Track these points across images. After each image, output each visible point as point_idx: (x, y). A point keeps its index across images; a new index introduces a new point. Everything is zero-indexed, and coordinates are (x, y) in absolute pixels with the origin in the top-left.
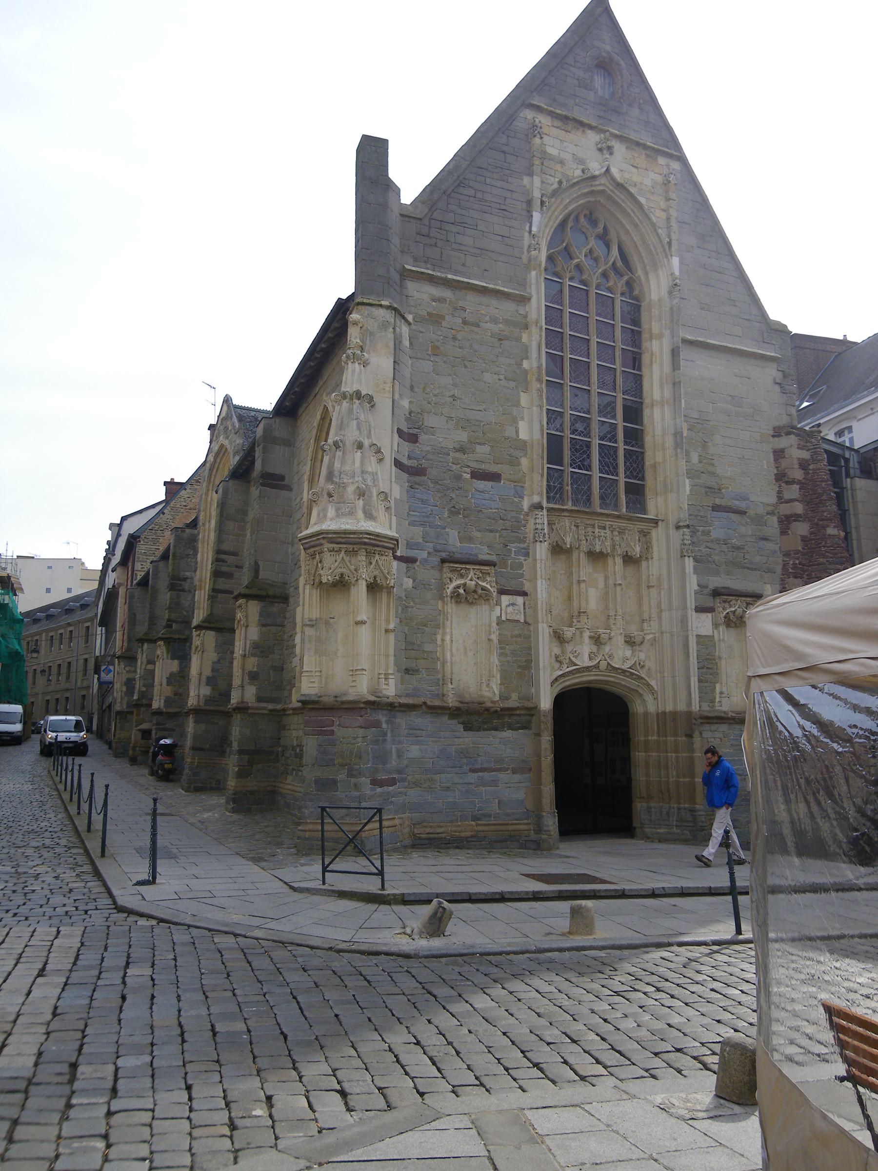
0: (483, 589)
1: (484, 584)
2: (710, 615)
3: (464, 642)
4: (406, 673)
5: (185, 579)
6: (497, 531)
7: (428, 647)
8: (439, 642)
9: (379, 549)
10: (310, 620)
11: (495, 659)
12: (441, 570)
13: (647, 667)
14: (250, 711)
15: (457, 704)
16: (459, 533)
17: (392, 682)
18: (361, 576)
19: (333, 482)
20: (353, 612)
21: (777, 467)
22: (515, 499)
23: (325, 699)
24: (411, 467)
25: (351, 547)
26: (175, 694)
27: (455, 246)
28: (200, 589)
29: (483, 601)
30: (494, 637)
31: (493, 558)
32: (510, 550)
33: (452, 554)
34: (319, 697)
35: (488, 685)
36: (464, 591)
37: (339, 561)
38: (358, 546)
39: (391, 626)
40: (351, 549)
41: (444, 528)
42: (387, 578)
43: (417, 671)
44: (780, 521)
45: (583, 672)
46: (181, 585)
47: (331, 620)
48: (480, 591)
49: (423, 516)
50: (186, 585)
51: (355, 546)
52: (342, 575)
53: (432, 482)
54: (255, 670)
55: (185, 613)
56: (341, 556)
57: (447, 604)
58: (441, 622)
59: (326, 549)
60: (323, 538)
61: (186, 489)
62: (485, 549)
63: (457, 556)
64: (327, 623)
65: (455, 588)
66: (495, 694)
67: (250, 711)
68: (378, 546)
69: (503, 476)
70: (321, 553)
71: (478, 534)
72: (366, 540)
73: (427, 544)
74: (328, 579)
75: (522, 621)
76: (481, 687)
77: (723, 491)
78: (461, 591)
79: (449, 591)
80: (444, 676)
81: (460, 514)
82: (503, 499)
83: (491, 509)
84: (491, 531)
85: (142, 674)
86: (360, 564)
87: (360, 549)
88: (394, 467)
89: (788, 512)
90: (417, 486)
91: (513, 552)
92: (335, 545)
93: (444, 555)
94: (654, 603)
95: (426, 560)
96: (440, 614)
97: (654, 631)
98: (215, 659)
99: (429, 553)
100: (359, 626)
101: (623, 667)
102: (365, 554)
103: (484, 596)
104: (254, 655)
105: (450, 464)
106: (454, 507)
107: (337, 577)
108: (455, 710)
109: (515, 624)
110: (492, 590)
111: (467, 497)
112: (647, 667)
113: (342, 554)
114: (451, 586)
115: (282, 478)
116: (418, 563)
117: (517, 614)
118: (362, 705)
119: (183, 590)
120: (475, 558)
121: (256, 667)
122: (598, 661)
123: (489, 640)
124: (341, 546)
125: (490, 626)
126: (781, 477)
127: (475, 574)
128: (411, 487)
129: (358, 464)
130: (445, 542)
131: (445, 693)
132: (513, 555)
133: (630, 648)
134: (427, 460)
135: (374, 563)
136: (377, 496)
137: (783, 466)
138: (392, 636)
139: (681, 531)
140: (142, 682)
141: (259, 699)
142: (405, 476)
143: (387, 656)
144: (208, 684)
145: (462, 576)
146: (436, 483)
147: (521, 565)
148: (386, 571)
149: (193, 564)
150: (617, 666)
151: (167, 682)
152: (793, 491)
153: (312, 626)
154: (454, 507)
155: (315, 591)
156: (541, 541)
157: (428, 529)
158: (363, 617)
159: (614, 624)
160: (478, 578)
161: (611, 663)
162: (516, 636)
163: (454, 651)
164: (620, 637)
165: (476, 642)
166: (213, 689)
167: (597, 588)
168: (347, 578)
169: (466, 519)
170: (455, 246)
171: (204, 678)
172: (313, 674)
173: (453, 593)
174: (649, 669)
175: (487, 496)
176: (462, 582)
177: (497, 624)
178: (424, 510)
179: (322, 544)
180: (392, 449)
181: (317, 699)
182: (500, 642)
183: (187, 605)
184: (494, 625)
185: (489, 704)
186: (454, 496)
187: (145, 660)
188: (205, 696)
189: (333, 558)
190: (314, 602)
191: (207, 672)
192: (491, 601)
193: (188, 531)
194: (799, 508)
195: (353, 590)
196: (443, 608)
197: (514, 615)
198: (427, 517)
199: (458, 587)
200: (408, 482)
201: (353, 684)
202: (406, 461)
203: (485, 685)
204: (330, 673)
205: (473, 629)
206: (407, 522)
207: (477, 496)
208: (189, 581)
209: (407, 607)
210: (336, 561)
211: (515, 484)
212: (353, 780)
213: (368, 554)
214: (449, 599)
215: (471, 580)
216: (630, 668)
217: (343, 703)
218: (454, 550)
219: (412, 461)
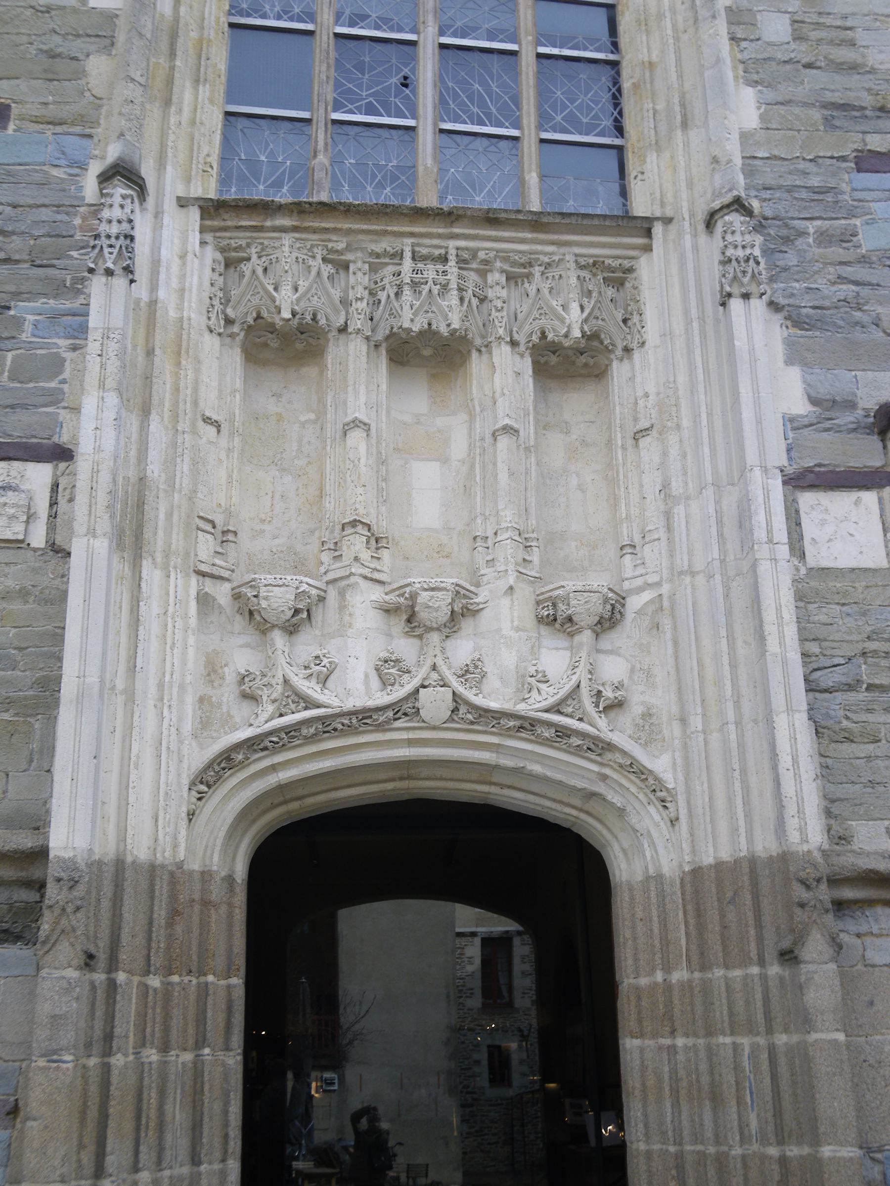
2: (869, 498)
13: (636, 710)
22: (55, 172)
45: (350, 730)
69: (15, 110)
75: (38, 538)
91: (28, 327)
94: (652, 482)
97: (653, 579)
101: (521, 708)
112: (636, 710)
122: (408, 688)
133: (566, 644)
147: (56, 365)
150: (494, 705)
156: (109, 273)
159: (491, 562)
161: (469, 695)
164: (505, 602)
167: (444, 460)
174: (647, 715)
211: (59, 129)
216: (556, 709)
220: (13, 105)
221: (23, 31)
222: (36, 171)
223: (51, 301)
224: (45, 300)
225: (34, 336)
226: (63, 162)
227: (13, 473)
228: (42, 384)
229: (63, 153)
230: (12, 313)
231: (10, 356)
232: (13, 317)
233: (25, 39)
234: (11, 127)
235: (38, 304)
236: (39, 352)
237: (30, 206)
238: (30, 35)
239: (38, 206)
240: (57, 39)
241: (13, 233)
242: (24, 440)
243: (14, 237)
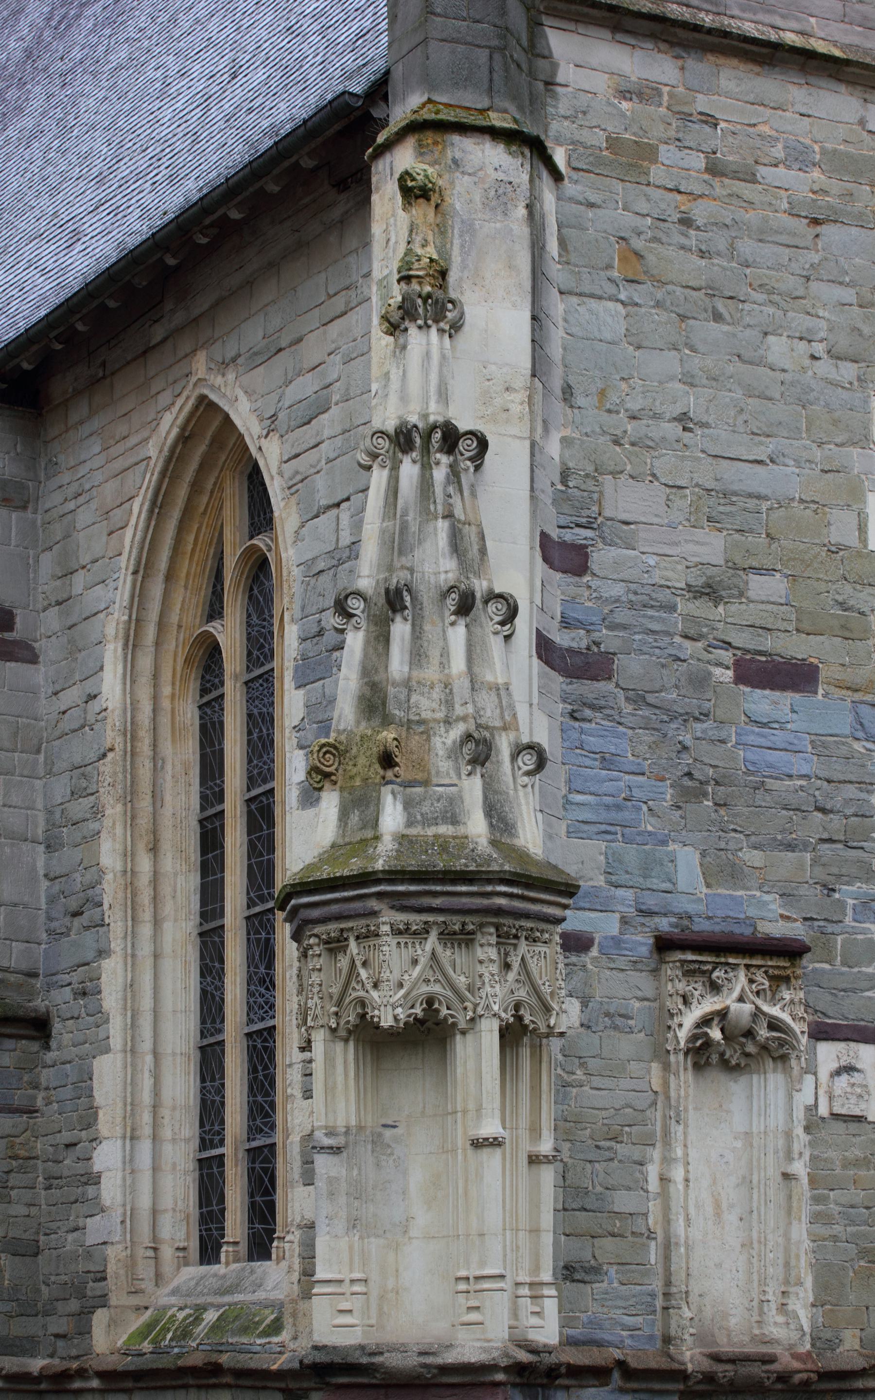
0: (774, 1025)
1: (775, 1011)
3: (714, 1182)
4: (565, 1278)
6: (805, 846)
7: (623, 1201)
8: (653, 1185)
9: (529, 924)
10: (331, 1133)
11: (800, 1231)
12: (655, 971)
15: (707, 1365)
16: (703, 854)
17: (551, 1306)
18: (488, 1007)
19: (387, 721)
20: (465, 1112)
22: (857, 746)
24: (570, 650)
29: (770, 1064)
30: (800, 1168)
31: (797, 930)
32: (842, 904)
33: (686, 922)
34: (373, 1354)
35: (782, 1308)
36: (722, 1030)
37: (423, 961)
38: (477, 919)
39: (546, 1147)
40: (457, 928)
41: (664, 843)
42: (548, 1009)
43: (595, 1271)
47: (388, 1133)
48: (763, 1033)
49: (607, 807)
51: (467, 919)
52: (430, 1001)
53: (627, 699)
56: (428, 947)
57: (677, 1074)
58: (658, 1128)
59: (386, 928)
60: (380, 895)
62: (774, 905)
63: (702, 926)
64: (377, 1141)
65: (698, 1025)
66: (804, 1335)
68: (527, 916)
69: (823, 675)
70: (368, 936)
71: (754, 857)
72: (502, 901)
73: (620, 892)
74: (396, 1018)
76: (761, 1313)
78: (716, 1034)
79: (683, 1035)
80: (668, 1283)
81: (705, 795)
82: (824, 745)
83: (790, 776)
84: (790, 847)
86: (481, 969)
87: (482, 926)
88: (535, 660)
90: (588, 713)
91: (849, 911)
93: (664, 924)
95: (617, 942)
96: (654, 1103)
99: (624, 921)
100: (486, 1151)
102: (493, 940)
103: (773, 1045)
105: (678, 639)
106: (689, 774)
107: (418, 1011)
108: (699, 1382)
109: (853, 1127)
110: (797, 1027)
111: (723, 742)
113: (432, 940)
114: (690, 1018)
116: (594, 952)
117: (860, 1096)
118: (500, 1377)
123: (786, 1176)
124: (431, 918)
125: (789, 1135)
127: (751, 981)
128: (572, 715)
129: (458, 664)
130: (667, 886)
131: (673, 1333)
132: (848, 920)
134: (612, 627)
135: (516, 966)
136: (514, 757)
138: (548, 1175)
142: (558, 681)
143: (535, 1231)
145: (715, 988)
146: (638, 699)
148: (546, 990)
153: (335, 1150)
154: (689, 774)
155: (339, 1046)
157: (618, 845)
158: (491, 1128)
160: (758, 993)
162: (856, 1163)
163: (692, 1211)
165: (746, 1182)
168: (444, 1012)
169: (722, 812)
172: (345, 1288)
173: (694, 1038)
175: (779, 738)
176: (718, 1007)
177: (807, 1129)
178: (608, 787)
179: (374, 914)
180: (532, 602)
181: (364, 1360)
182: (813, 1181)
184: (799, 1131)
185: (786, 1362)
186: (688, 740)
189: (407, 954)
190: (340, 1079)
192: (793, 1062)
195: (462, 1047)
196: (666, 1084)
197: (854, 1099)
198: (618, 807)
199: (706, 1021)
200: (564, 701)
201: (474, 1317)
202: (561, 639)
203: (773, 1306)
204: (391, 1284)
205: (739, 1144)
206: (564, 828)
207: (751, 739)
209: (566, 1085)
210: (415, 962)
211: (858, 696)
213: (505, 939)
214: (681, 1057)
215: (741, 999)
217: (445, 1369)
218: (691, 908)
219: (573, 633)
220: (820, 665)
221: (821, 576)
222: (843, 744)
223: (864, 886)
224: (859, 884)
225: (855, 920)
226: (860, 734)
227: (851, 1053)
228: (864, 969)
229: (861, 724)
230: (837, 896)
231: (839, 939)
232: (839, 900)
233: (822, 587)
234: (821, 691)
235: (854, 888)
236: (860, 937)
237: (840, 782)
238: (827, 582)
239: (845, 782)
240: (848, 588)
241: (831, 811)
242: (856, 1023)
243: (832, 816)
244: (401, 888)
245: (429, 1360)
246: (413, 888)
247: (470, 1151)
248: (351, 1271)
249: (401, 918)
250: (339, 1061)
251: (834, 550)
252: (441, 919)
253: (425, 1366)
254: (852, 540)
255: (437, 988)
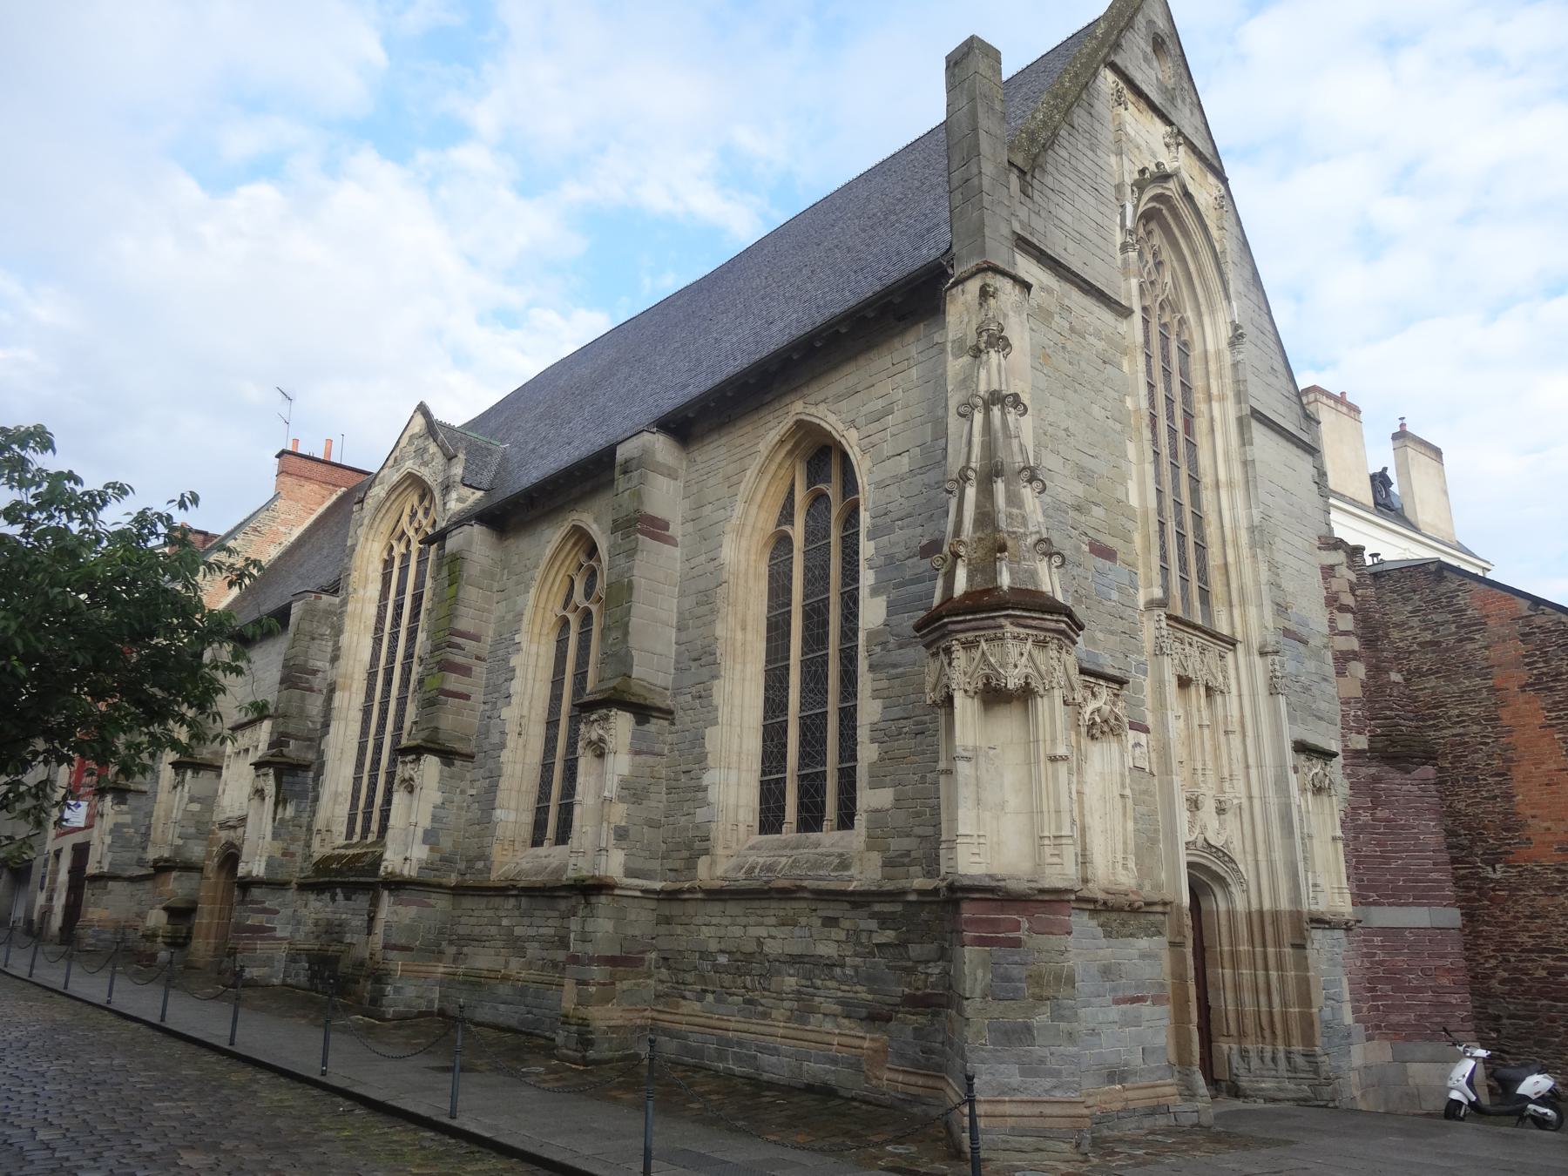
5: (314, 672)
14: (617, 892)
21: (1326, 588)
23: (1012, 885)
25: (1041, 635)
26: (284, 854)
27: (1056, 222)
28: (343, 689)
38: (1051, 635)
44: (1336, 659)
46: (307, 681)
47: (992, 752)
50: (317, 682)
51: (1048, 634)
54: (623, 824)
55: (310, 724)
61: (236, 539)
67: (617, 892)
69: (1118, 556)
75: (1147, 770)
77: (1289, 611)
85: (179, 818)
89: (1344, 648)
92: (1022, 630)
98: (439, 801)
104: (621, 799)
107: (1022, 682)
115: (666, 526)
119: (311, 690)
120: (1101, 670)
121: (624, 820)
124: (1030, 631)
126: (1332, 601)
137: (1334, 588)
139: (1270, 658)
140: (178, 830)
141: (630, 873)
144: (424, 842)
149: (329, 650)
151: (274, 833)
152: (1346, 622)
153: (968, 759)
158: (1061, 750)
166: (432, 850)
170: (1056, 222)
171: (420, 833)
179: (1001, 627)
181: (994, 884)
183: (314, 713)
187: (186, 795)
188: (419, 860)
191: (425, 822)
193: (324, 597)
194: (1354, 644)
195: (1042, 705)
205: (1097, 778)
208: (320, 675)
212: (1063, 1025)
240: (1124, 519)
244: (1018, 613)
245: (1033, 885)
246: (1025, 614)
247: (1048, 763)
248: (979, 830)
249: (1017, 630)
250: (969, 710)
251: (1119, 501)
252: (1035, 633)
253: (1031, 889)
254: (1124, 498)
255: (1030, 671)
